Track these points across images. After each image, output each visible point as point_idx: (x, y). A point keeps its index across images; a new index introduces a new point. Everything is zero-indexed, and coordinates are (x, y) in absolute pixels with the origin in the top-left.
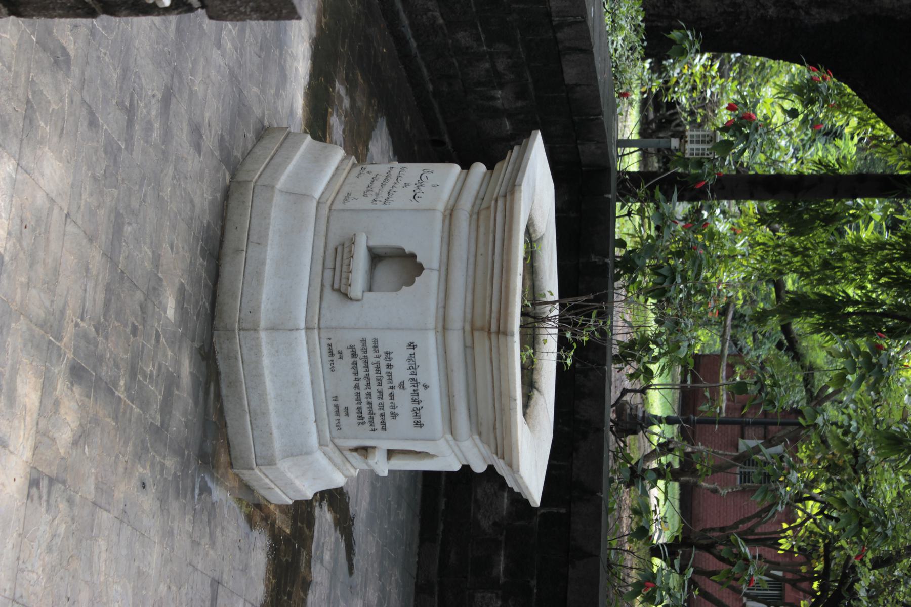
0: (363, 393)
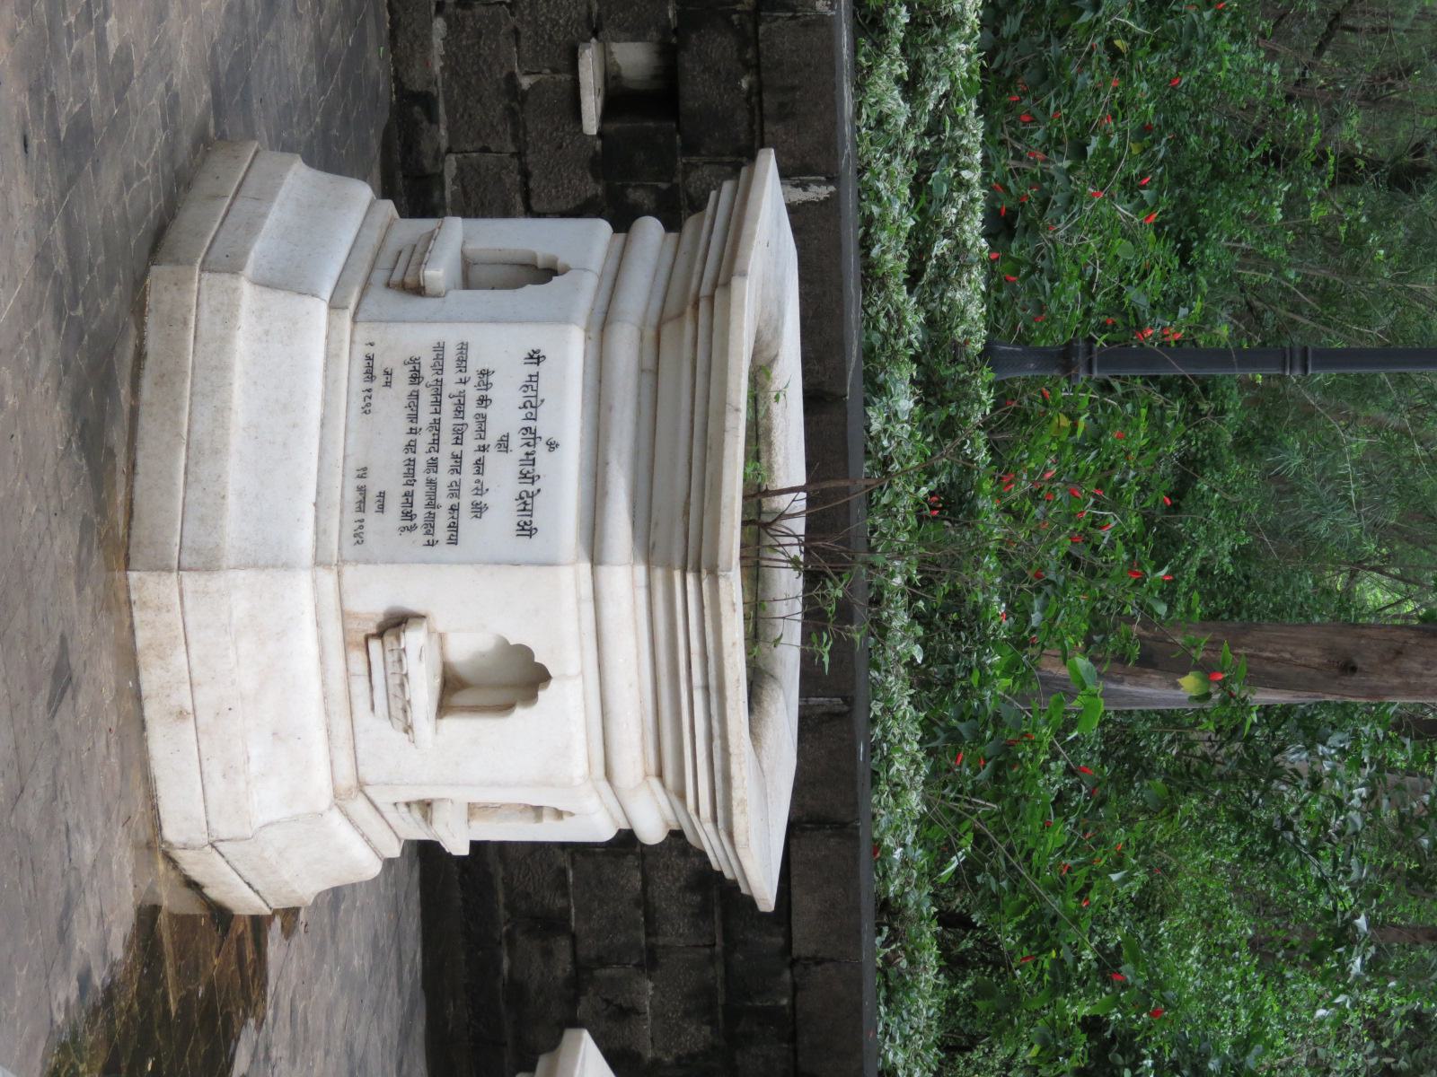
0: (422, 459)
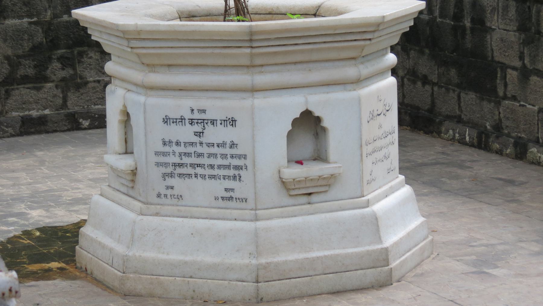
0: (208, 172)
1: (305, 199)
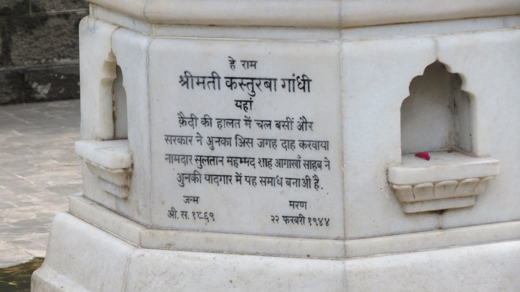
0: (260, 171)
1: (432, 221)
